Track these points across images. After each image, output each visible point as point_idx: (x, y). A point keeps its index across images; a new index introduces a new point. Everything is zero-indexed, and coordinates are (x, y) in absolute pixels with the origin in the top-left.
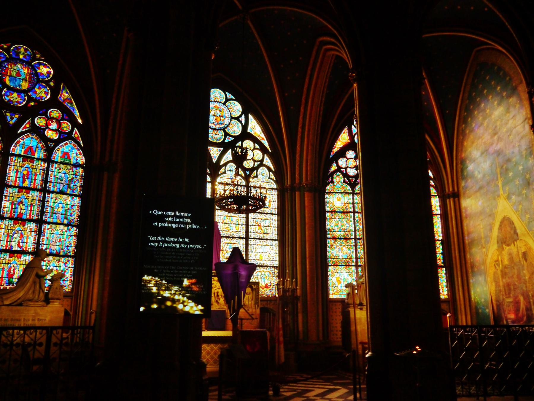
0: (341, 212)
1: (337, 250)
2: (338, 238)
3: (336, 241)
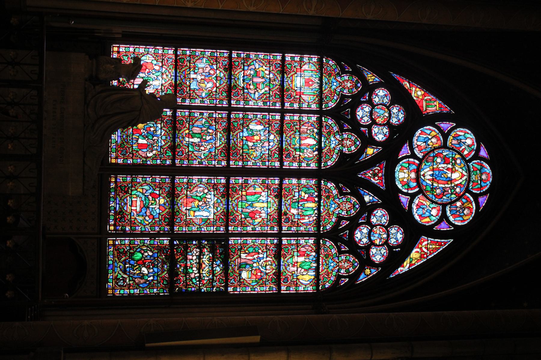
0: (282, 85)
1: (207, 71)
2: (230, 75)
3: (226, 70)
